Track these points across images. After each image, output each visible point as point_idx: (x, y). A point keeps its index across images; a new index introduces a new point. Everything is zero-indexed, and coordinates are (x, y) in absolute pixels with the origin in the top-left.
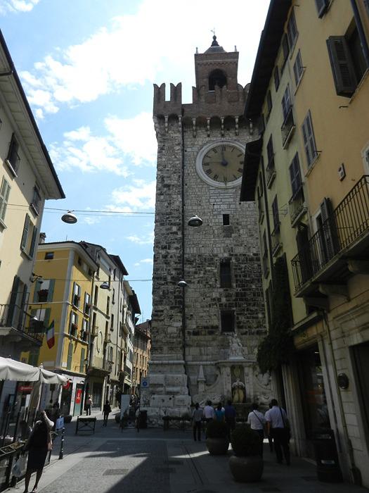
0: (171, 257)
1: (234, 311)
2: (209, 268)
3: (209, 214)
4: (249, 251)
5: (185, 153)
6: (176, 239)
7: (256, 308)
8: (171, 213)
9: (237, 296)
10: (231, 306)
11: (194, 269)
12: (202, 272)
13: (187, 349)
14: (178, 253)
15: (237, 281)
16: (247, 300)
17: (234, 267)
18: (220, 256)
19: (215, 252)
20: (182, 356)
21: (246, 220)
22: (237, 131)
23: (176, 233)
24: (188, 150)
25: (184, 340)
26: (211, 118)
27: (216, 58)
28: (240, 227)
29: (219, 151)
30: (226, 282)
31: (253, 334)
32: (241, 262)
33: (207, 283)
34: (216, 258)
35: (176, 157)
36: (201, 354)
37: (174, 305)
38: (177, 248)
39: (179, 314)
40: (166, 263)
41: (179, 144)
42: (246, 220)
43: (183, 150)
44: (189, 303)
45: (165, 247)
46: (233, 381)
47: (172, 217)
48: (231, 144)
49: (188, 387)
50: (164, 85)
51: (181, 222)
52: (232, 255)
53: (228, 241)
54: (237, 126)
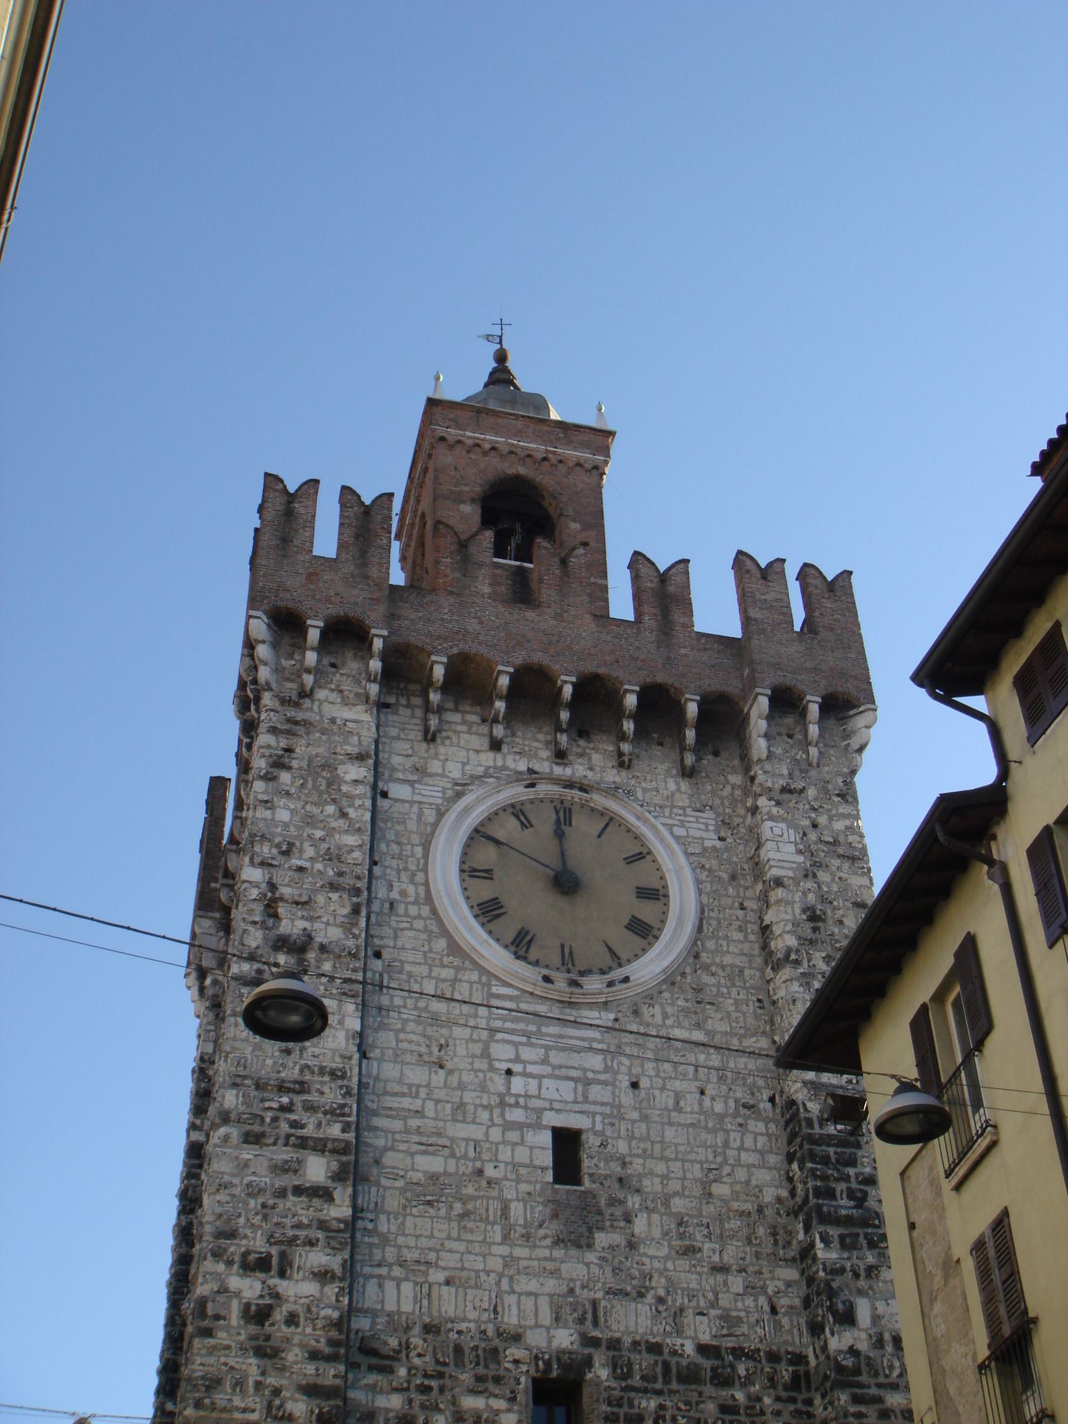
3: (484, 1116)
4: (680, 1333)
5: (383, 804)
6: (322, 1225)
8: (302, 1087)
18: (536, 1339)
19: (511, 1319)
21: (660, 1168)
22: (626, 747)
23: (322, 1193)
24: (399, 791)
26: (517, 671)
27: (518, 434)
28: (633, 1201)
29: (544, 822)
34: (514, 1352)
35: (344, 815)
38: (323, 1276)
40: (260, 1353)
41: (360, 758)
42: (660, 1168)
45: (262, 1264)
47: (310, 1108)
48: (599, 800)
50: (312, 485)
51: (350, 1136)
52: (594, 1342)
53: (575, 1268)
54: (629, 726)
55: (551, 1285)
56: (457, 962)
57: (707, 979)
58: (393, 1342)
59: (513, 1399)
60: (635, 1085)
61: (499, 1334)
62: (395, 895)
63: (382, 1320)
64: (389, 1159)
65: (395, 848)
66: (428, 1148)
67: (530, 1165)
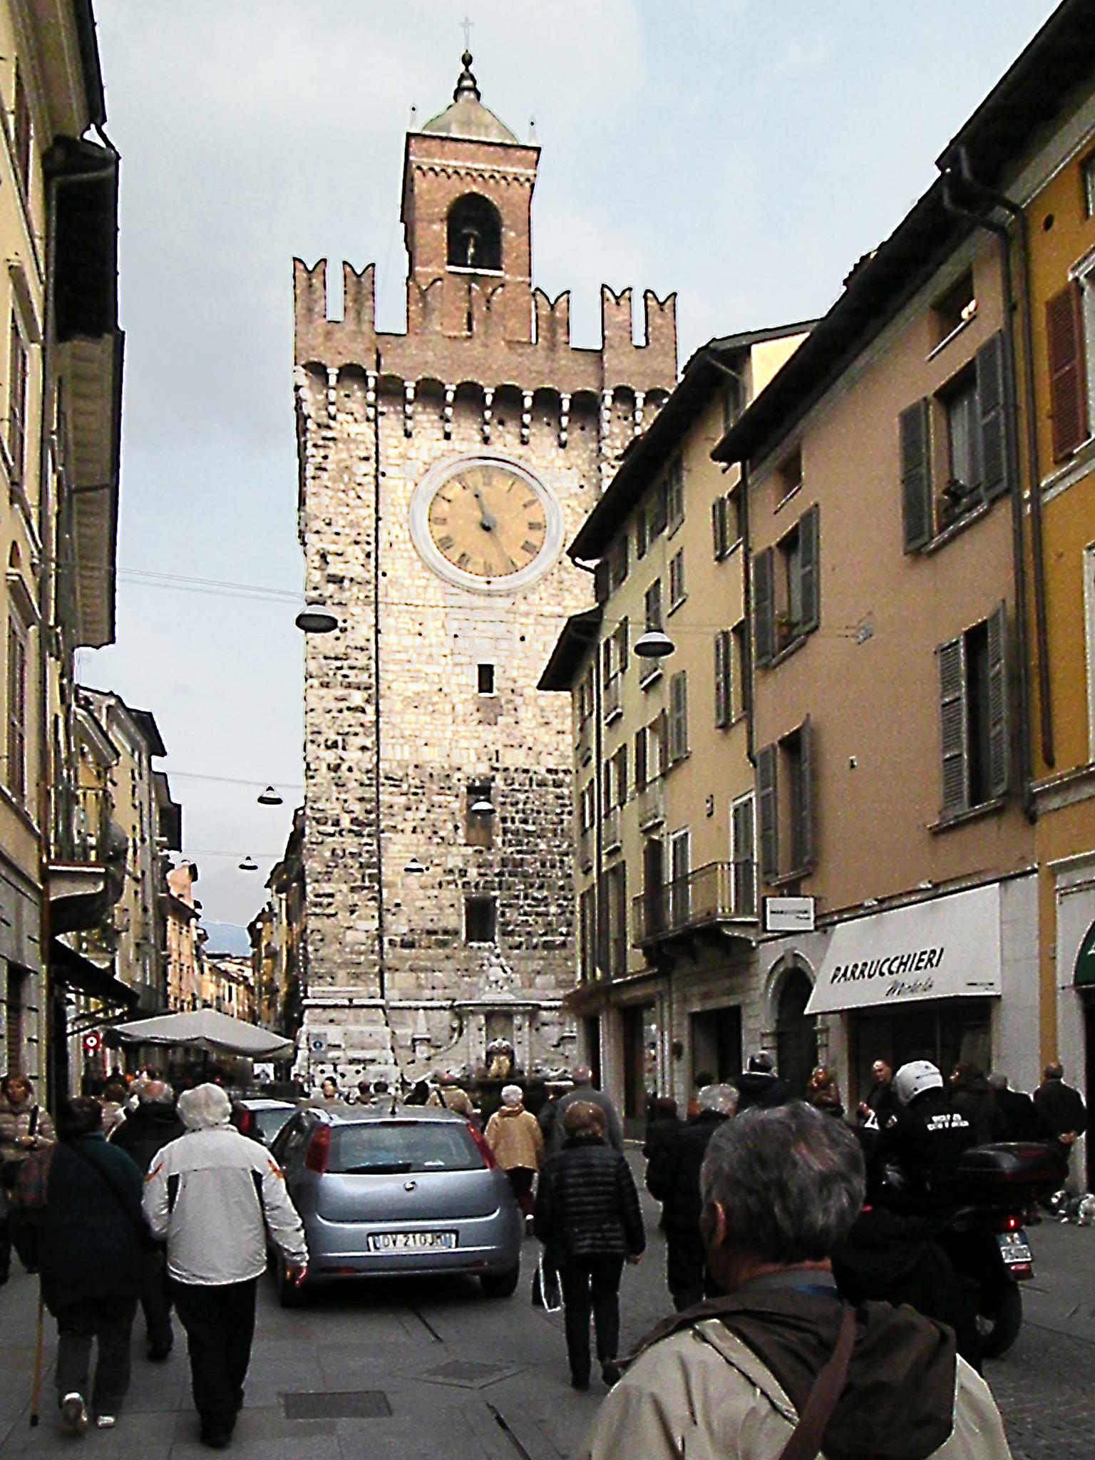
0: (350, 769)
1: (495, 898)
2: (442, 798)
6: (362, 725)
7: (545, 893)
9: (504, 866)
10: (489, 886)
11: (403, 799)
12: (423, 807)
13: (386, 975)
14: (367, 760)
15: (505, 831)
16: (526, 875)
17: (502, 799)
18: (468, 769)
19: (456, 762)
20: (379, 990)
25: (382, 958)
26: (458, 386)
28: (518, 700)
30: (479, 823)
31: (535, 947)
32: (516, 786)
33: (435, 833)
34: (458, 775)
36: (420, 986)
37: (359, 883)
39: (372, 903)
40: (337, 785)
43: (378, 474)
44: (390, 878)
46: (491, 1037)
49: (393, 1049)
52: (497, 770)
53: (487, 733)
55: (476, 743)
56: (427, 575)
57: (565, 576)
58: (401, 774)
59: (457, 796)
60: (523, 639)
61: (451, 767)
62: (392, 538)
63: (395, 764)
64: (394, 686)
65: (392, 509)
66: (414, 679)
67: (467, 685)
